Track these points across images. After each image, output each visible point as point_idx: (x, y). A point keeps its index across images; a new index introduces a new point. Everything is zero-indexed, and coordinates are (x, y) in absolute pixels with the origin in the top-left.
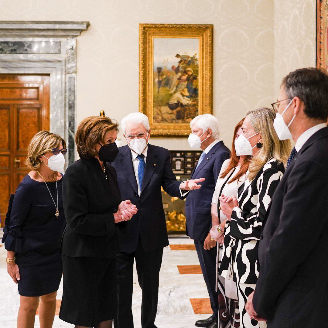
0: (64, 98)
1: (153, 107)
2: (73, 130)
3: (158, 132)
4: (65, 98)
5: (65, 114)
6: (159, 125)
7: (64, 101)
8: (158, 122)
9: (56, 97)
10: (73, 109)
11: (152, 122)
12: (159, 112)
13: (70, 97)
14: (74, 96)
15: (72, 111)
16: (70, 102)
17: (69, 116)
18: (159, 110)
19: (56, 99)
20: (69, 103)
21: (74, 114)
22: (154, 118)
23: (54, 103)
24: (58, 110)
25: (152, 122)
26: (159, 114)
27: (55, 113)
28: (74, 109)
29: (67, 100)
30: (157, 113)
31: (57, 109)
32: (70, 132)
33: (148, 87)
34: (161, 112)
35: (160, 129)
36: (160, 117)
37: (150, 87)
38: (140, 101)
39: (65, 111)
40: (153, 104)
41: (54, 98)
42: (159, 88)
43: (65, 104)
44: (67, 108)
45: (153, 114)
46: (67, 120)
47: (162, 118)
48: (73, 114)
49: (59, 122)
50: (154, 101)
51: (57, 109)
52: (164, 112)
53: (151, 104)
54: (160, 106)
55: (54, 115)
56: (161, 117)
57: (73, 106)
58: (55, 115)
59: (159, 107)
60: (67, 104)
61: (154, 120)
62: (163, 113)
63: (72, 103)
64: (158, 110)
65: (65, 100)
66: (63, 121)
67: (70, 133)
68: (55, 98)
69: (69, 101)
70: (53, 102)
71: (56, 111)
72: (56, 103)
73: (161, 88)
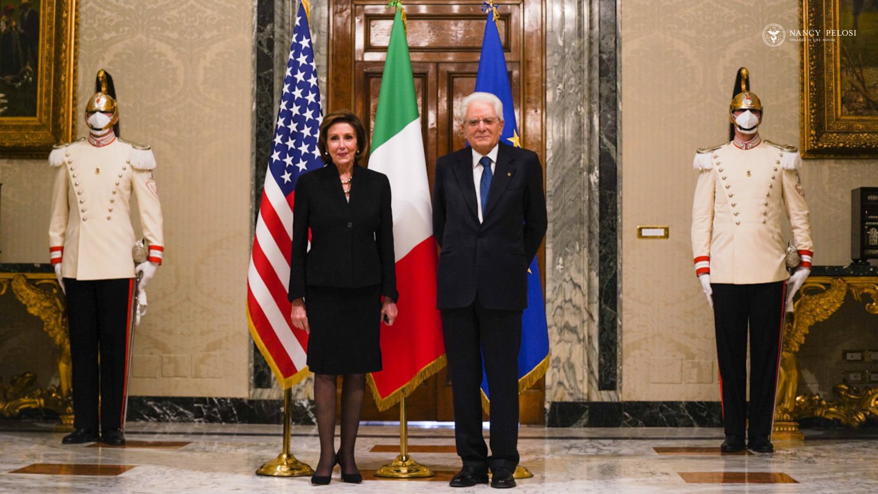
0: (586, 44)
1: (842, 69)
2: (613, 136)
3: (858, 139)
4: (591, 44)
5: (590, 89)
6: (858, 120)
7: (586, 54)
8: (856, 114)
9: (564, 41)
10: (610, 74)
11: (839, 113)
12: (858, 84)
13: (603, 42)
14: (614, 39)
15: (608, 82)
16: (605, 57)
17: (600, 95)
18: (858, 78)
19: (564, 47)
20: (601, 61)
21: (616, 91)
22: (843, 102)
23: (557, 57)
24: (568, 79)
25: (839, 113)
26: (857, 90)
27: (561, 86)
28: (616, 75)
29: (596, 50)
30: (853, 86)
31: (565, 76)
32: (605, 140)
33: (827, 13)
34: (863, 83)
35: (863, 133)
36: (861, 100)
37: (832, 11)
38: (802, 51)
39: (590, 81)
40: (842, 62)
41: (559, 46)
42: (856, 14)
43: (590, 62)
44: (596, 74)
45: (842, 90)
46: (595, 107)
47: (868, 100)
48: (614, 89)
49: (573, 114)
50: (843, 53)
51: (565, 76)
52: (871, 84)
53: (835, 62)
54: (860, 67)
55: (558, 91)
56: (864, 96)
57: (611, 67)
58: (561, 94)
59: (858, 71)
60: (596, 62)
61: (844, 107)
62: (869, 87)
63: (609, 60)
64: (855, 78)
65: (590, 51)
66: (583, 110)
67: (605, 146)
68: (561, 43)
69: (600, 52)
70: (556, 55)
71: (564, 80)
72: (563, 58)
73: (862, 17)
